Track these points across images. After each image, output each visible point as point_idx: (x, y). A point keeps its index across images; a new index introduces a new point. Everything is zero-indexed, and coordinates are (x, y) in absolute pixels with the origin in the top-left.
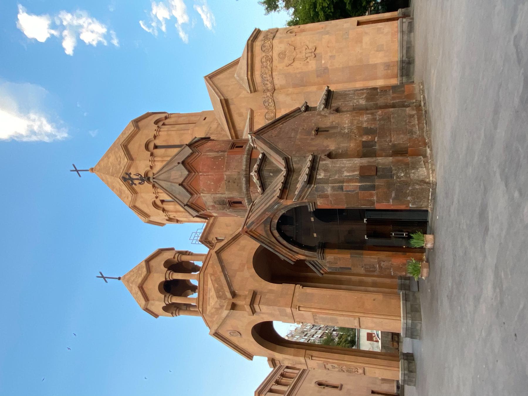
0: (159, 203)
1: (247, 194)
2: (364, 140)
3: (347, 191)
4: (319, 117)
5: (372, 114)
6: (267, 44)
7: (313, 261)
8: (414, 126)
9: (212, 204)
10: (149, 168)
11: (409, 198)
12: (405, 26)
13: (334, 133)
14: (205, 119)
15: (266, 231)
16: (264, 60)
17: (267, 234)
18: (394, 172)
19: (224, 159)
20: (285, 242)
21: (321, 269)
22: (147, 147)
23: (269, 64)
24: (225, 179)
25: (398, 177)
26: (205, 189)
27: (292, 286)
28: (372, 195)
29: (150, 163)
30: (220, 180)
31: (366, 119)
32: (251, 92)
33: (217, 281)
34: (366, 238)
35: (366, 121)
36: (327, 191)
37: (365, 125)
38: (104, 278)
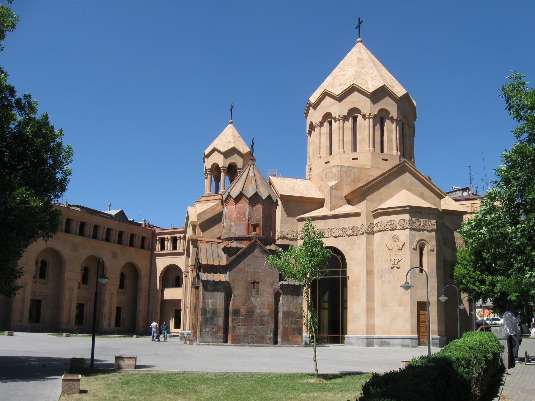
2: (242, 310)
4: (271, 281)
5: (269, 315)
6: (405, 223)
8: (252, 338)
12: (408, 342)
13: (251, 292)
14: (383, 160)
16: (393, 222)
18: (210, 326)
19: (244, 221)
23: (389, 227)
25: (205, 328)
30: (231, 220)
31: (264, 311)
32: (373, 212)
33: (212, 208)
35: (261, 312)
37: (258, 311)
38: (231, 110)
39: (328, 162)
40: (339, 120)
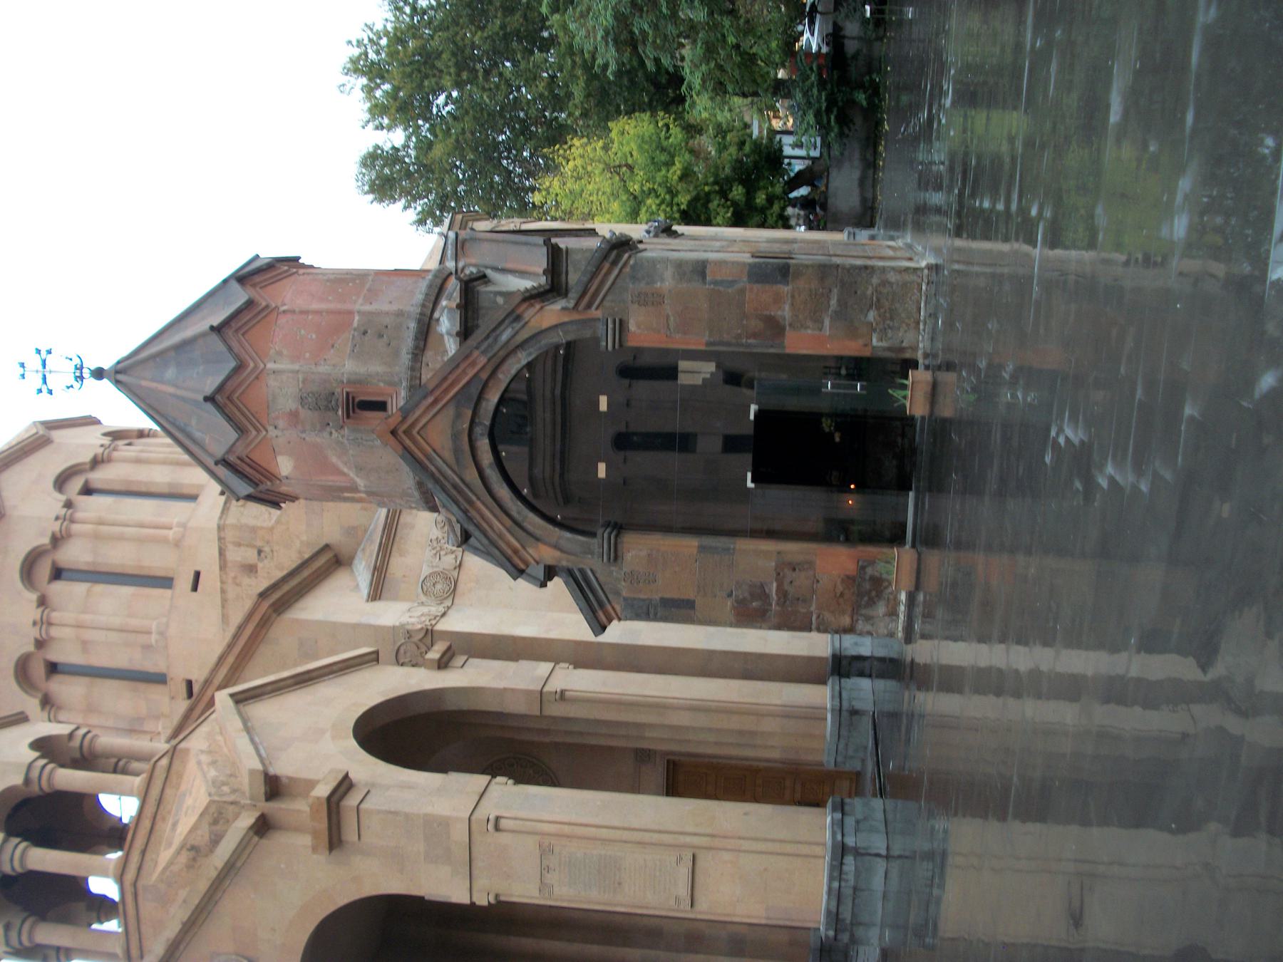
0: (38, 670)
1: (412, 369)
3: (715, 283)
7: (582, 571)
9: (292, 405)
10: (46, 540)
11: (872, 315)
15: (455, 437)
17: (457, 451)
20: (504, 492)
21: (601, 605)
22: (61, 482)
24: (355, 324)
26: (285, 352)
27: (478, 781)
28: (778, 300)
29: (56, 527)
34: (750, 485)
36: (662, 280)
39: (197, 575)
40: (72, 521)
